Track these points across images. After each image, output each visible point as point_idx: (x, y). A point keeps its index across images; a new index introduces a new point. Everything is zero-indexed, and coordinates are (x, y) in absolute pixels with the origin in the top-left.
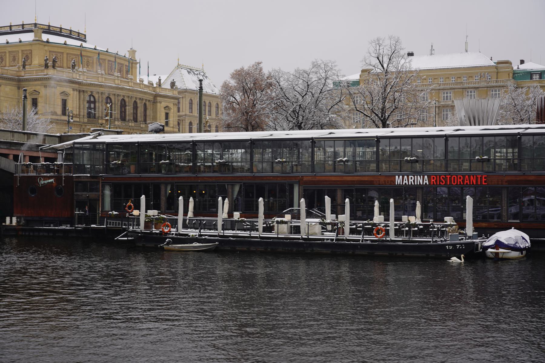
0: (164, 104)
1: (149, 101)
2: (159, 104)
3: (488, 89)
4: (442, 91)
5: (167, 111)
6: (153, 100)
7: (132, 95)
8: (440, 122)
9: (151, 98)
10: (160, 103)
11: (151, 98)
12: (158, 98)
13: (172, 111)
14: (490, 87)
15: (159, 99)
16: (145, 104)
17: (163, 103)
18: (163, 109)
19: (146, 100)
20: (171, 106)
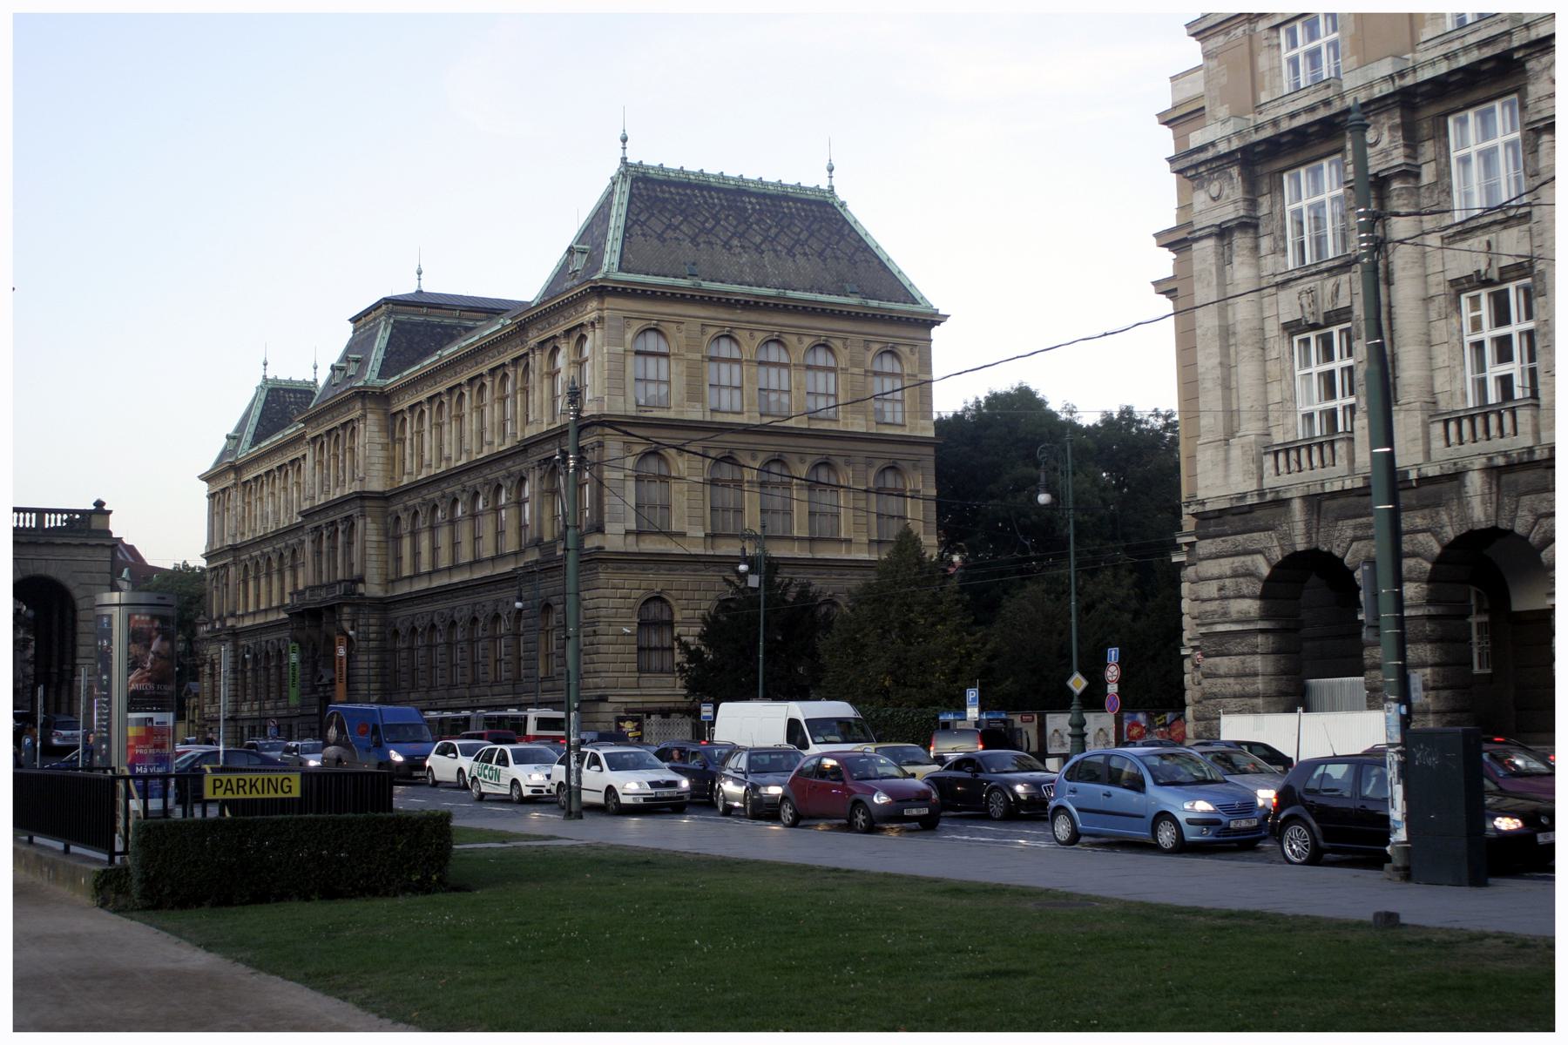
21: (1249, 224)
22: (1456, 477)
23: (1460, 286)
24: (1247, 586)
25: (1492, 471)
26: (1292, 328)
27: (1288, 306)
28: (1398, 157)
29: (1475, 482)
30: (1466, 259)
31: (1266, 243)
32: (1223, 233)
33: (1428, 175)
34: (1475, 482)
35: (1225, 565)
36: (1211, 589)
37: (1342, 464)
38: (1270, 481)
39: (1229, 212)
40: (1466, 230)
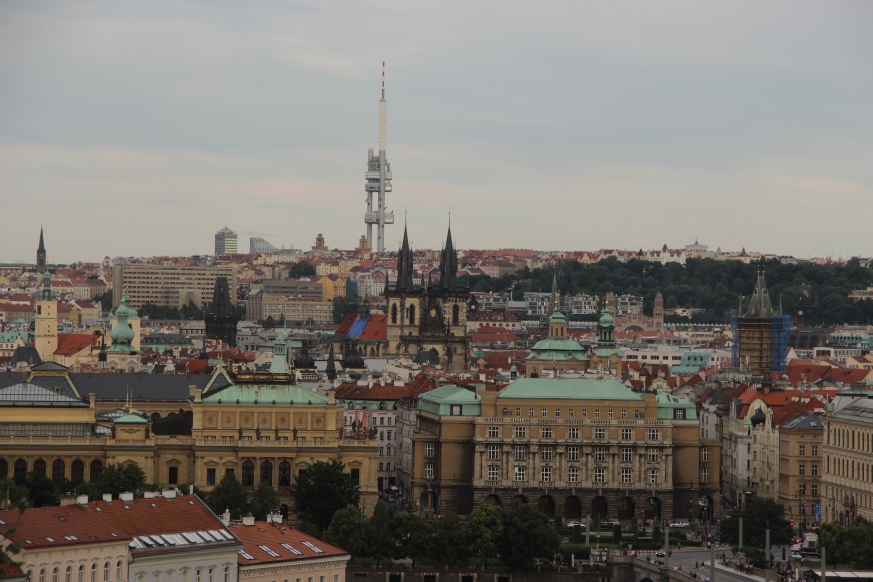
8: (593, 462)
22: (517, 489)
23: (515, 466)
24: (483, 498)
25: (523, 489)
26: (488, 466)
27: (490, 463)
28: (511, 451)
29: (520, 490)
30: (516, 464)
32: (481, 453)
33: (513, 453)
34: (520, 490)
35: (480, 495)
37: (500, 485)
38: (488, 485)
39: (482, 450)
40: (517, 461)
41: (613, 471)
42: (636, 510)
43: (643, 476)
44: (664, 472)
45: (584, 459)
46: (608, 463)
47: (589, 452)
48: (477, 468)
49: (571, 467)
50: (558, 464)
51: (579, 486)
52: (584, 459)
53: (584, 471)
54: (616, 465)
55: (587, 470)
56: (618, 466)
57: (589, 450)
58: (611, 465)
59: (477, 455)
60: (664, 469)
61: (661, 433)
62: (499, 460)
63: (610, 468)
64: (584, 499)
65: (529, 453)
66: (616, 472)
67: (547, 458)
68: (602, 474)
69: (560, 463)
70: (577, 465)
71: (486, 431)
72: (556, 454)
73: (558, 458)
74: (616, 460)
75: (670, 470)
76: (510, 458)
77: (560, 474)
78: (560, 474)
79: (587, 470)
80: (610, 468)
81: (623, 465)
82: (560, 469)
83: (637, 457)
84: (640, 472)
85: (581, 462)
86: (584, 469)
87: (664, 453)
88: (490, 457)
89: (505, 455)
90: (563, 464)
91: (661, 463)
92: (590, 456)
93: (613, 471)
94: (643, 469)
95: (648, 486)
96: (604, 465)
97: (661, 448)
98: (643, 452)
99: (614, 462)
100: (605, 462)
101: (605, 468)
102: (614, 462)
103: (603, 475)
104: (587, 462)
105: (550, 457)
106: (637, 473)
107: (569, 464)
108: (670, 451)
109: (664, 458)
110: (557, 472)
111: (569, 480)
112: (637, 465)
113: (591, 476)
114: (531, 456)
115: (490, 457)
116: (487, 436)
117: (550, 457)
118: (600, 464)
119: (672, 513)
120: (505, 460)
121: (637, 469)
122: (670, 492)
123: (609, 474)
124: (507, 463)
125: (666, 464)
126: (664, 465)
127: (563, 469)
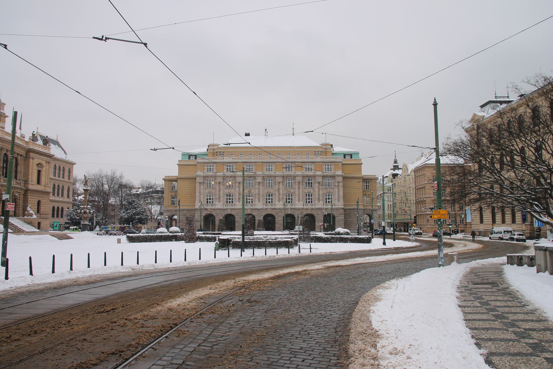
0: (37, 161)
1: (21, 155)
2: (31, 160)
3: (323, 163)
4: (285, 163)
5: (40, 169)
6: (25, 155)
7: (2, 146)
8: (284, 188)
9: (23, 153)
10: (33, 159)
11: (23, 153)
12: (31, 154)
13: (44, 168)
14: (324, 162)
15: (32, 154)
16: (16, 159)
17: (35, 160)
18: (35, 166)
19: (18, 154)
20: (44, 163)
21: (203, 183)
31: (204, 185)
36: (197, 216)
39: (202, 181)
41: (299, 195)
42: (316, 223)
43: (321, 198)
44: (337, 195)
45: (277, 187)
46: (295, 189)
47: (280, 181)
48: (197, 194)
49: (268, 193)
50: (257, 191)
51: (274, 207)
52: (277, 187)
53: (277, 196)
54: (301, 190)
55: (279, 194)
56: (303, 191)
57: (280, 179)
58: (297, 190)
59: (198, 184)
60: (337, 192)
61: (334, 166)
62: (214, 189)
63: (297, 193)
64: (277, 216)
65: (235, 183)
66: (301, 195)
67: (249, 186)
68: (291, 197)
69: (259, 189)
70: (272, 191)
71: (205, 167)
72: (256, 182)
73: (257, 186)
74: (301, 187)
75: (341, 194)
76: (222, 187)
77: (259, 198)
78: (259, 198)
79: (279, 194)
80: (297, 193)
81: (306, 191)
82: (259, 194)
83: (317, 185)
84: (319, 195)
85: (275, 189)
86: (277, 193)
87: (336, 181)
88: (207, 187)
89: (218, 184)
90: (261, 190)
91: (334, 188)
92: (281, 184)
93: (299, 195)
94: (321, 192)
95: (325, 205)
96: (292, 191)
97: (333, 177)
98: (320, 179)
99: (299, 188)
100: (293, 188)
101: (293, 193)
102: (299, 188)
103: (292, 198)
104: (279, 189)
105: (252, 186)
106: (317, 196)
107: (266, 191)
108: (340, 179)
109: (336, 184)
110: (257, 196)
111: (267, 203)
112: (317, 190)
113: (283, 199)
114: (237, 184)
115: (207, 187)
116: (205, 171)
117: (252, 186)
118: (289, 190)
119: (343, 225)
120: (218, 189)
121: (317, 193)
122: (343, 209)
123: (295, 197)
124: (219, 191)
125: (338, 189)
126: (336, 190)
127: (261, 194)
